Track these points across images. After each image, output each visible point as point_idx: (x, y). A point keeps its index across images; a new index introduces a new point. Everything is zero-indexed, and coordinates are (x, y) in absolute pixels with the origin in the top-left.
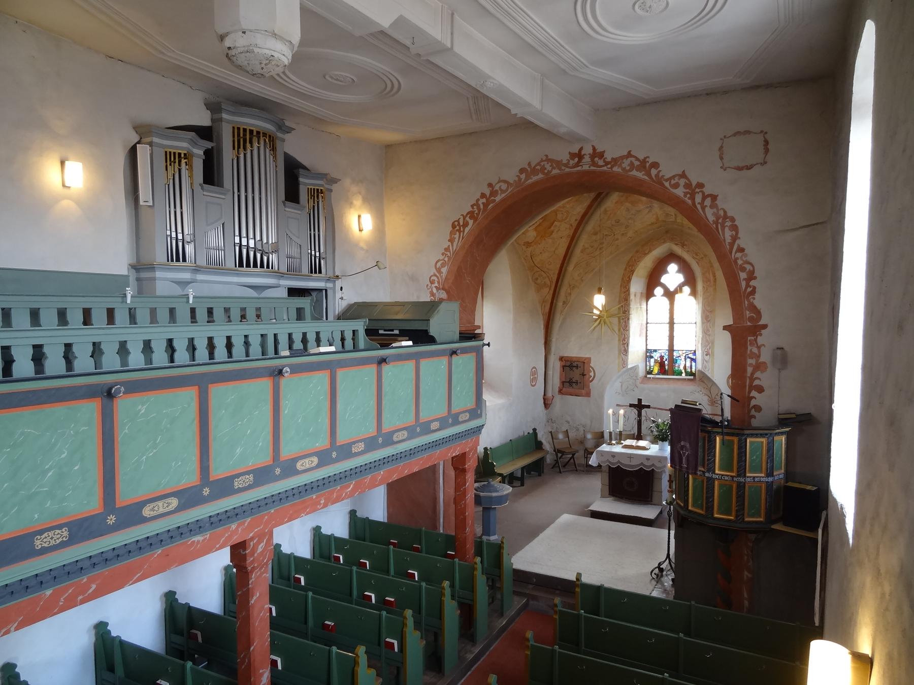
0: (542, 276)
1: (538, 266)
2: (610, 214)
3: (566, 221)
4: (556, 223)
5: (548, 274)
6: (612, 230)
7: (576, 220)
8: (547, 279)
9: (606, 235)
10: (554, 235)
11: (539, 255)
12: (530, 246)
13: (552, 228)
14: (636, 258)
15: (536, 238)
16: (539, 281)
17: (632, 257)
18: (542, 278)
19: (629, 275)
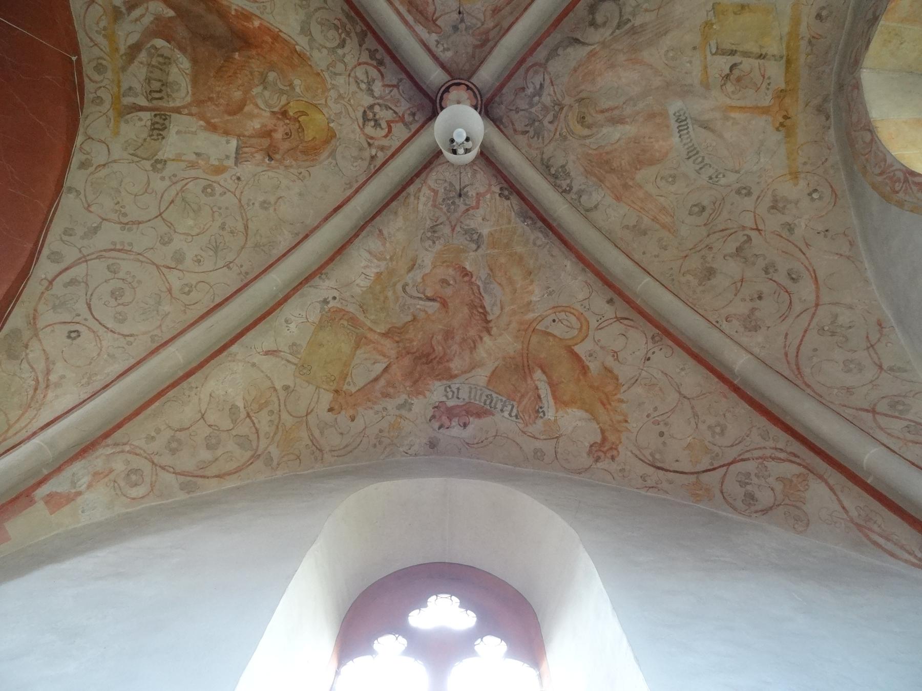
0: (748, 475)
1: (705, 464)
2: (655, 219)
3: (593, 323)
4: (577, 349)
5: (757, 453)
6: (723, 230)
7: (610, 301)
8: (771, 464)
9: (739, 249)
10: (624, 372)
11: (664, 443)
12: (614, 448)
13: (594, 367)
14: (877, 171)
15: (595, 418)
16: (765, 497)
17: (874, 187)
18: (755, 480)
19: (914, 188)
